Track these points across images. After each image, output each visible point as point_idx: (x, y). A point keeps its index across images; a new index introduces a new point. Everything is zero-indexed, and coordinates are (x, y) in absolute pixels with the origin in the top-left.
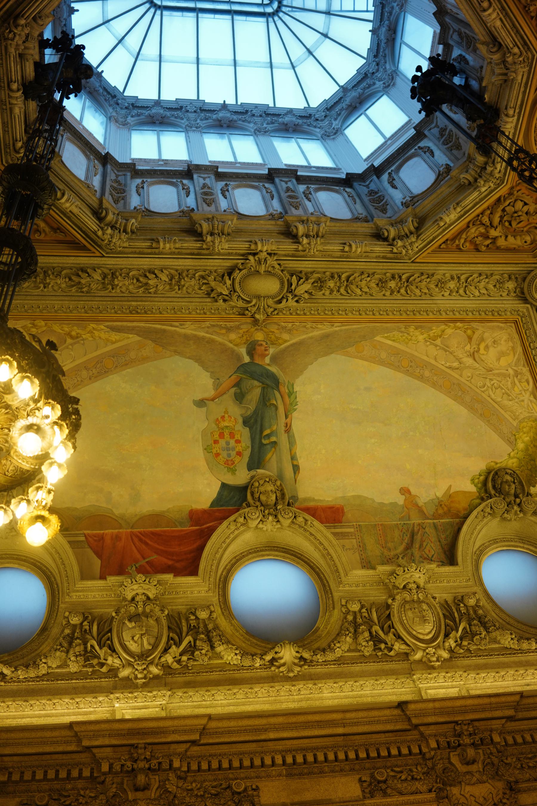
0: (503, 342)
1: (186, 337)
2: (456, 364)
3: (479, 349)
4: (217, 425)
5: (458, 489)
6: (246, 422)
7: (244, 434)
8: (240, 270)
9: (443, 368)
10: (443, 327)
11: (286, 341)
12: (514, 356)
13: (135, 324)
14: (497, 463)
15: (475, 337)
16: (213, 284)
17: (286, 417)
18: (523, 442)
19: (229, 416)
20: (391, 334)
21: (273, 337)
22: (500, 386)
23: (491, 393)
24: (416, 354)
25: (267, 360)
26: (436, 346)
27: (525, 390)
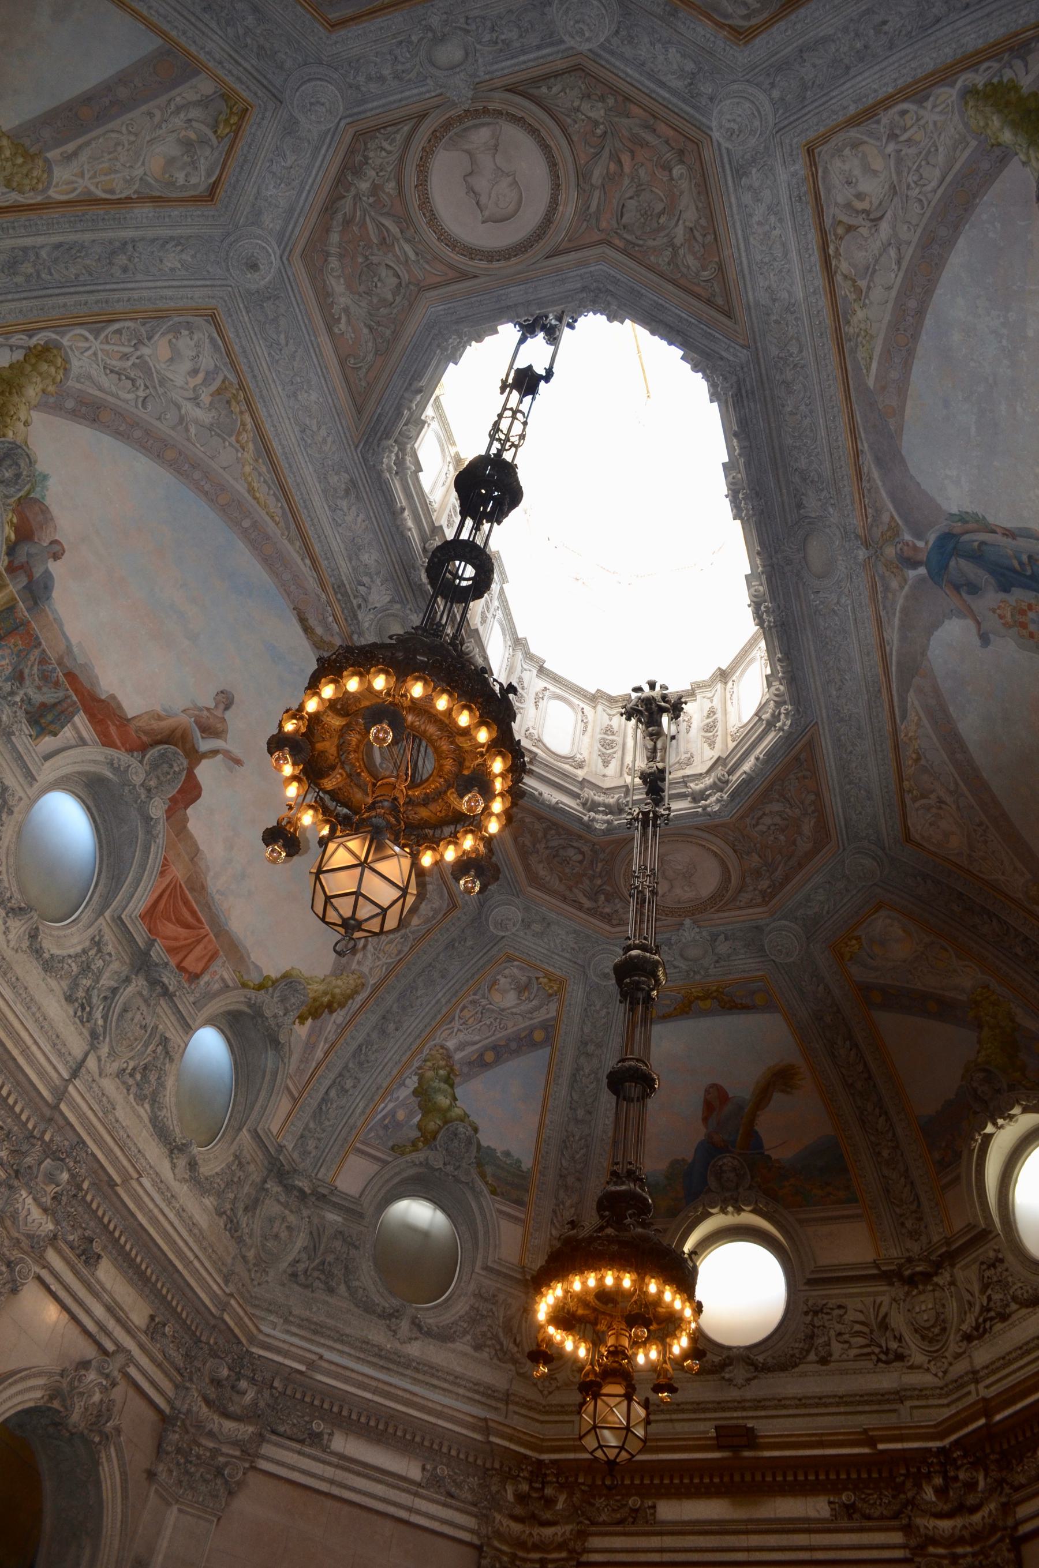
0: (847, 167)
1: (903, 639)
2: (892, 252)
3: (864, 211)
4: (1010, 627)
9: (901, 274)
10: (839, 278)
11: (892, 517)
12: (865, 142)
13: (895, 693)
15: (844, 218)
17: (994, 532)
18: (1001, 129)
19: (999, 607)
20: (862, 362)
21: (889, 534)
22: (917, 170)
23: (929, 188)
24: (886, 321)
25: (920, 544)
26: (869, 288)
27: (918, 120)
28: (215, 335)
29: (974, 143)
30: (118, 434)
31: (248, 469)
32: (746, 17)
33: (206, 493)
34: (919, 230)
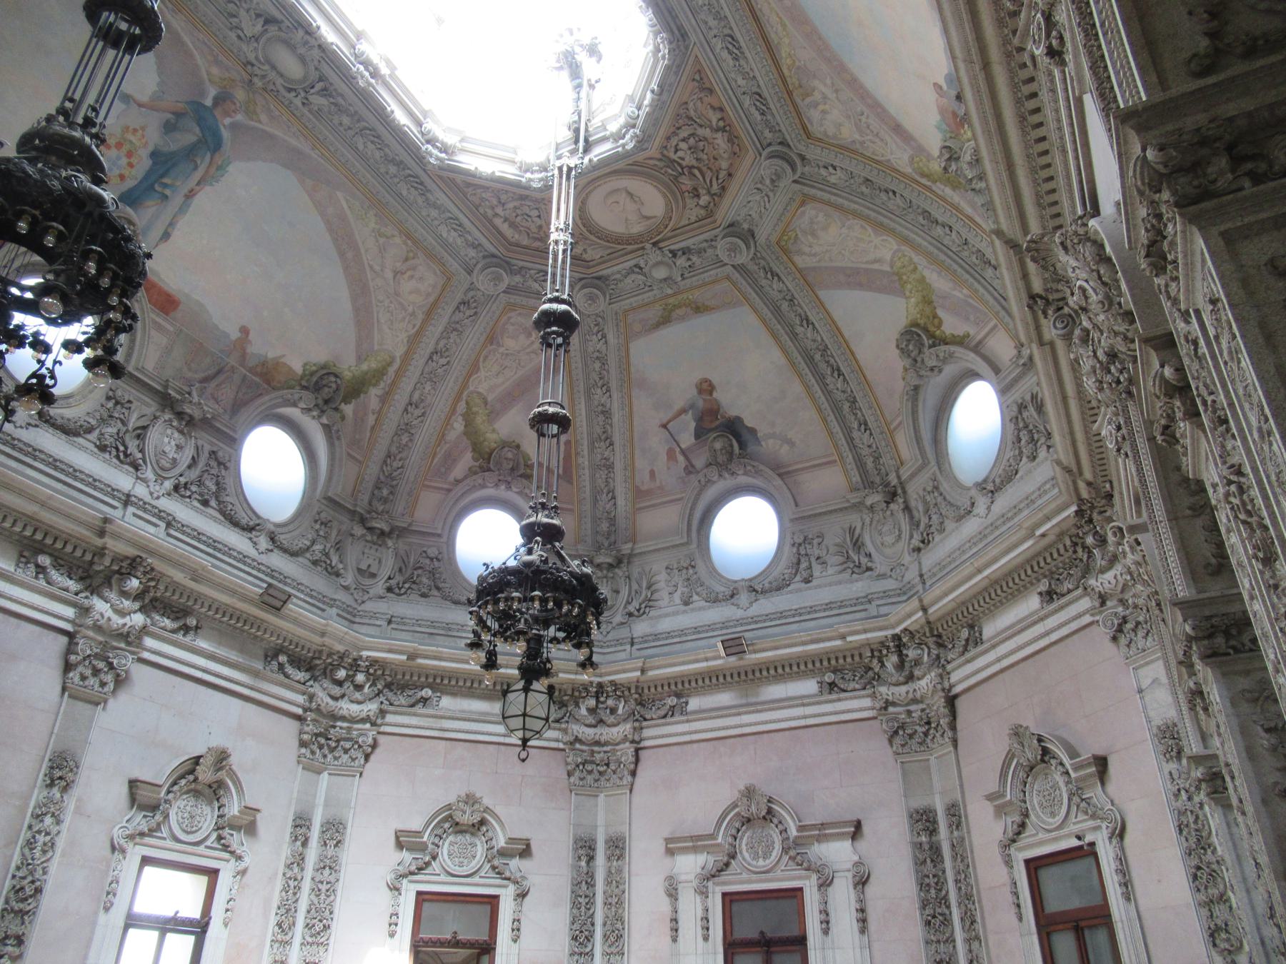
2: (377, 268)
6: (154, 155)
7: (143, 163)
8: (280, 29)
9: (366, 262)
10: (396, 233)
11: (260, 122)
16: (243, 13)
17: (198, 184)
19: (143, 136)
25: (227, 121)
28: (808, 125)
29: (376, 347)
30: (884, 110)
31: (786, 40)
32: (509, 318)
33: (820, 39)
34: (372, 289)
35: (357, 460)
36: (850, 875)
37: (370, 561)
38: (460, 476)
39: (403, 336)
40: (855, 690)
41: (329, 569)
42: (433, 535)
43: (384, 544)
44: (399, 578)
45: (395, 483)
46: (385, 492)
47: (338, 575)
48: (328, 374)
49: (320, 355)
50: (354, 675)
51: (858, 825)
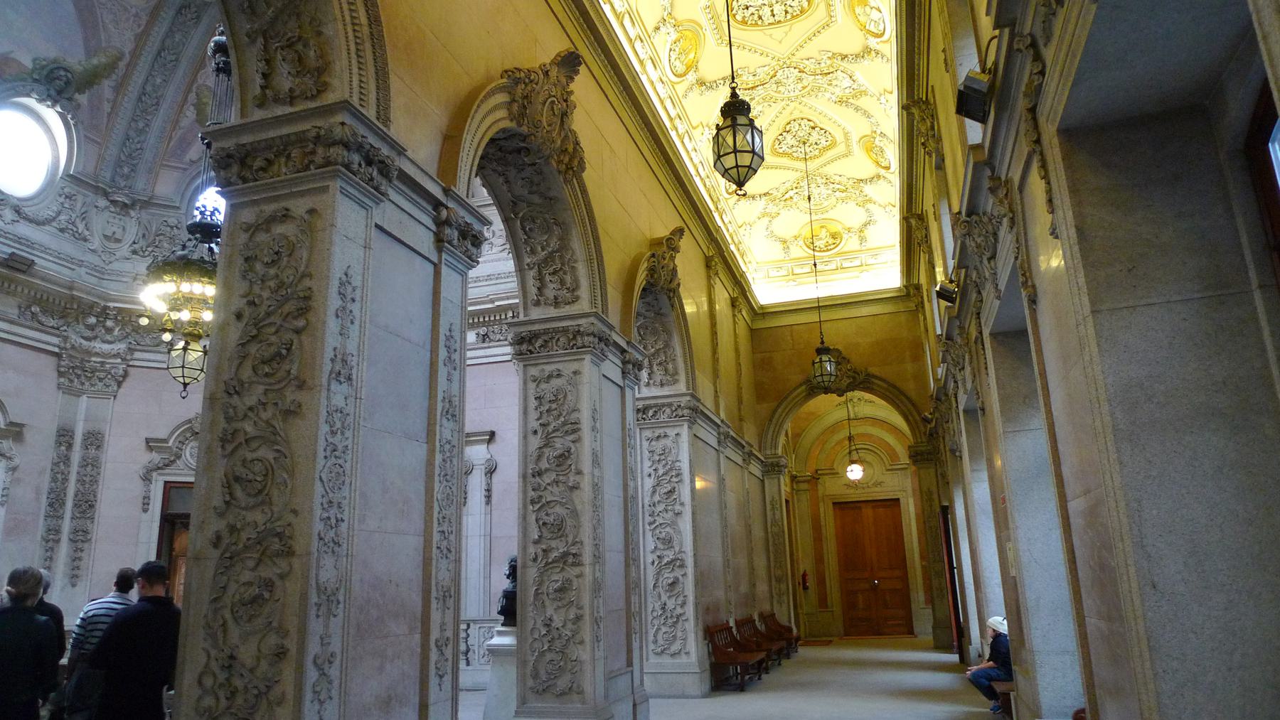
5: (18, 58)
14: (65, 60)
29: (104, 45)
35: (96, 142)
36: (483, 467)
37: (114, 229)
38: (194, 159)
39: (129, 35)
40: (499, 340)
41: (77, 235)
42: (174, 207)
43: (127, 214)
44: (142, 243)
45: (135, 162)
46: (126, 170)
47: (85, 240)
48: (58, 68)
49: (49, 52)
50: (106, 322)
51: (492, 434)
